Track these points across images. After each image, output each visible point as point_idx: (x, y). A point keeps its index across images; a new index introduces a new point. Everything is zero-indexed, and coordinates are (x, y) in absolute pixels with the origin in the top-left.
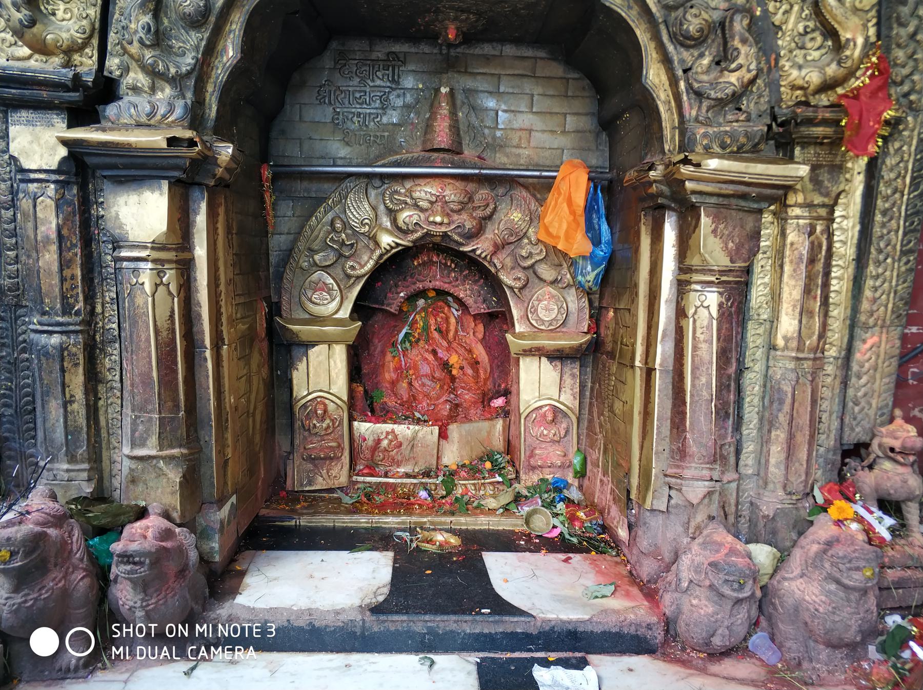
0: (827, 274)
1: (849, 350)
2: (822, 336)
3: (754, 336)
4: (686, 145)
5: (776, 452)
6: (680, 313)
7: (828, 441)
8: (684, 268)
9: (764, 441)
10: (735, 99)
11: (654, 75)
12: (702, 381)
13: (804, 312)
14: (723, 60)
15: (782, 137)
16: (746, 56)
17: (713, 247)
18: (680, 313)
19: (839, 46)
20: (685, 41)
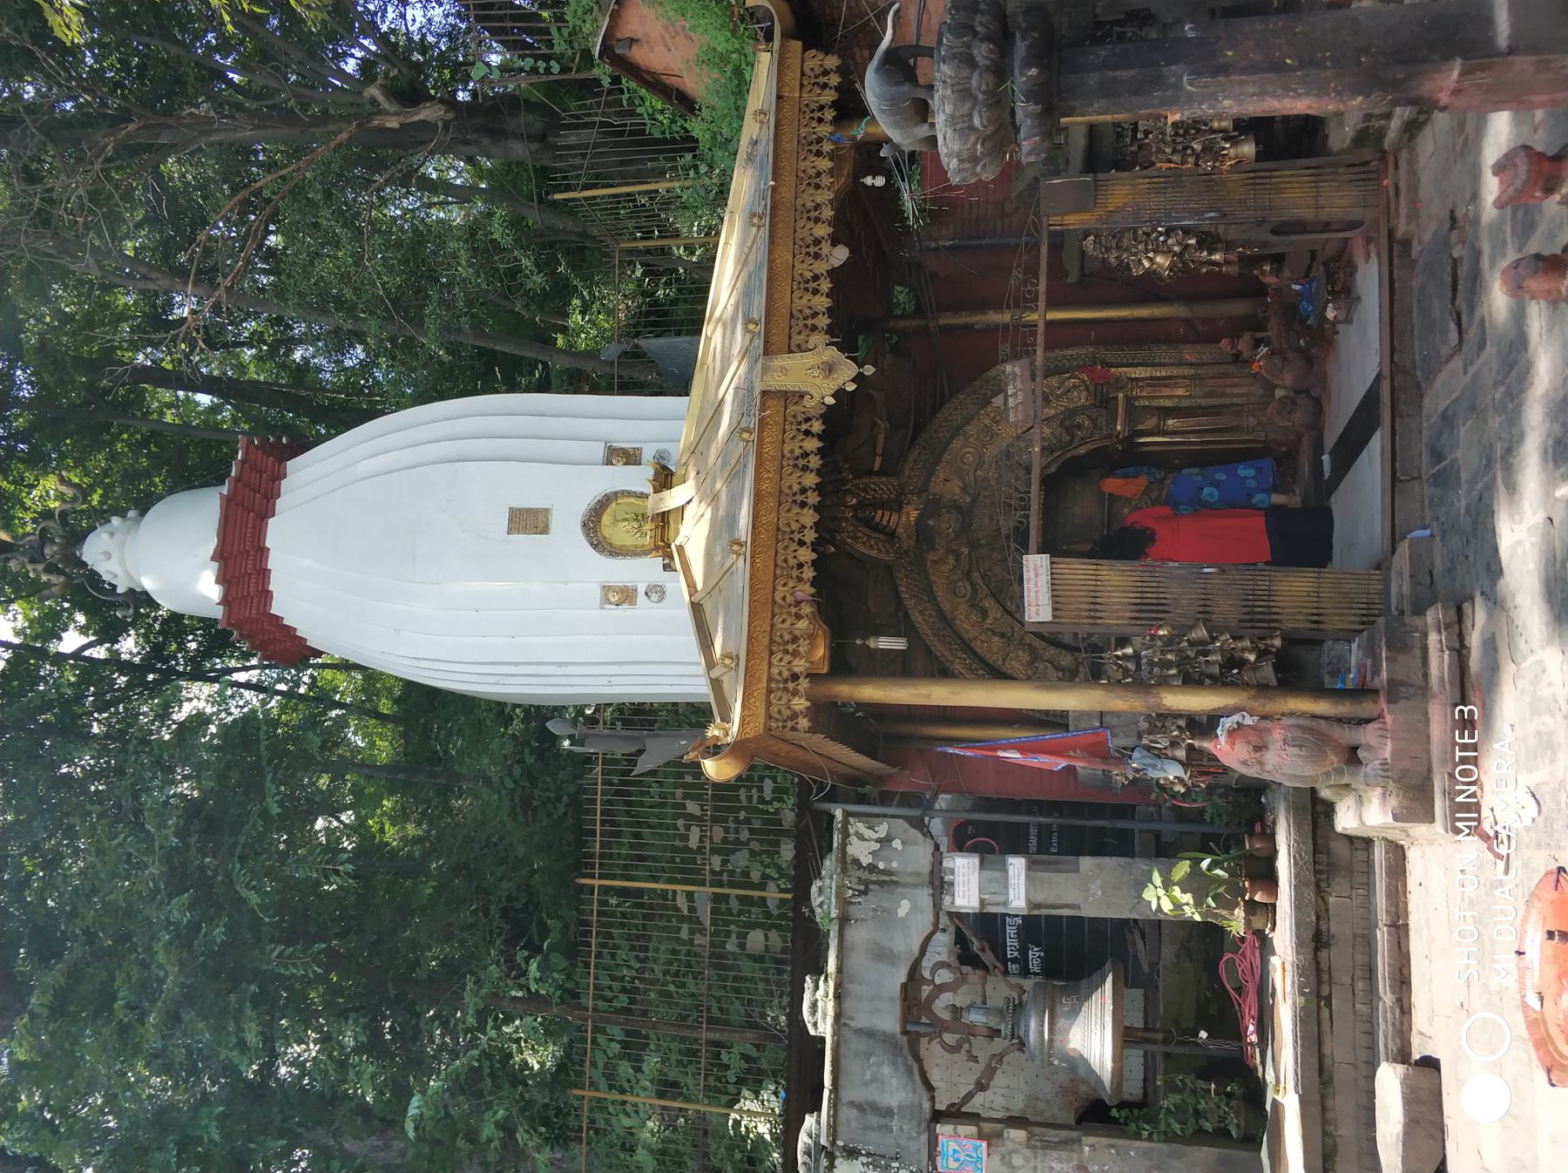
0: (1159, 378)
1: (1192, 365)
2: (1184, 377)
3: (1185, 403)
4: (1110, 437)
5: (1235, 391)
6: (1176, 433)
7: (1231, 368)
8: (1158, 435)
9: (1231, 396)
10: (1093, 421)
11: (1082, 451)
12: (1205, 422)
13: (1175, 386)
14: (1079, 427)
15: (1105, 403)
16: (1079, 420)
17: (1151, 423)
18: (1176, 433)
19: (1075, 387)
20: (1072, 441)
